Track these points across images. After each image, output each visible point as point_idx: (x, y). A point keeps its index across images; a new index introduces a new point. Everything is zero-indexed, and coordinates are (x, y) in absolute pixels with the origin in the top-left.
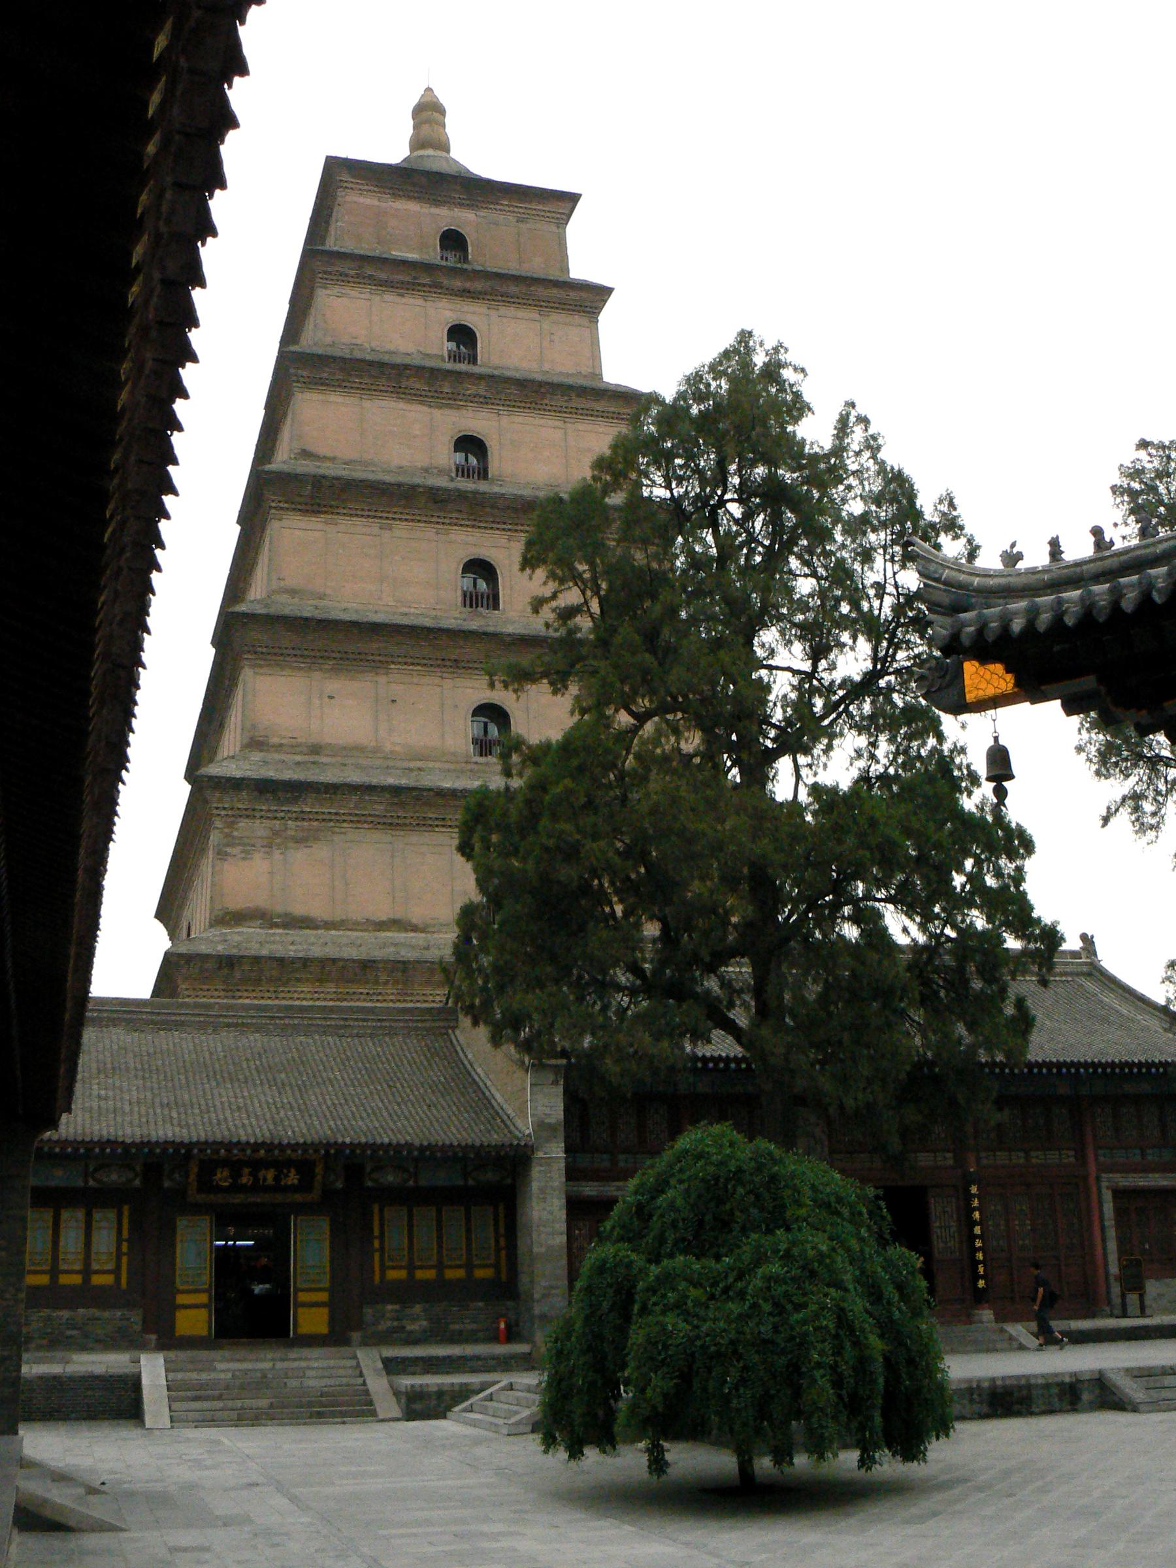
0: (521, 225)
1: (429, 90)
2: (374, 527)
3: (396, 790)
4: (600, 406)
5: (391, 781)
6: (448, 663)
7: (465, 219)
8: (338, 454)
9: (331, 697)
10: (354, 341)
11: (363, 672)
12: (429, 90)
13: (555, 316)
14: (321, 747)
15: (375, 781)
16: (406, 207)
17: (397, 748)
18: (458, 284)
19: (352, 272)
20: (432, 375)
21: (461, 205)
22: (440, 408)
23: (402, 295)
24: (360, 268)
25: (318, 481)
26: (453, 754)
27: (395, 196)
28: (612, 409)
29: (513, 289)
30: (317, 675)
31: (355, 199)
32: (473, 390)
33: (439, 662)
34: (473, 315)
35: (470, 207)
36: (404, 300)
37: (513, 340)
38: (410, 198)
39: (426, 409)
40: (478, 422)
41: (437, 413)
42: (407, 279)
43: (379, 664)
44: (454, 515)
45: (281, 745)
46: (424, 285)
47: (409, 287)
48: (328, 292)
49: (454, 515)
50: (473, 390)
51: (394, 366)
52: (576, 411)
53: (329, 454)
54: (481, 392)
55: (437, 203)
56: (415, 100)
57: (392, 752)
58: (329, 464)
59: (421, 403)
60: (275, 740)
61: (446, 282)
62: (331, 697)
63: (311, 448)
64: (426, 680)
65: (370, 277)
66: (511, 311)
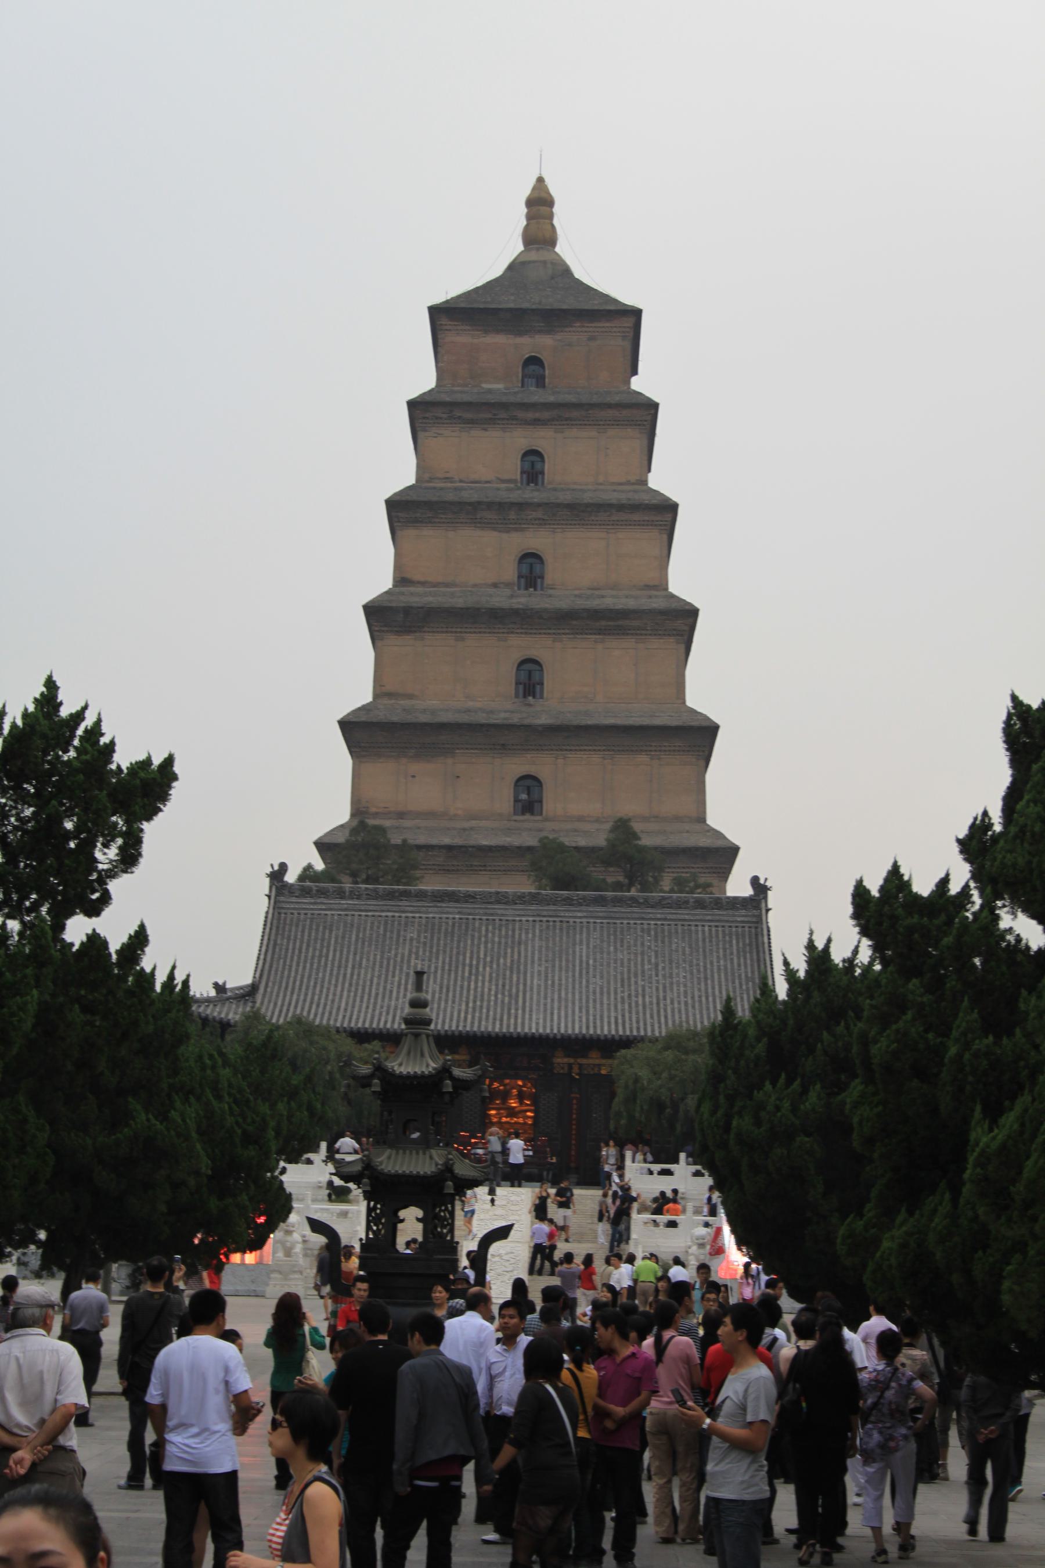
1: (540, 180)
3: (450, 848)
4: (636, 517)
5: (447, 841)
7: (542, 344)
9: (413, 776)
10: (448, 475)
12: (540, 180)
15: (434, 841)
17: (460, 812)
18: (530, 415)
20: (501, 507)
21: (540, 332)
22: (508, 532)
23: (485, 430)
25: (407, 611)
27: (486, 332)
28: (646, 518)
29: (575, 414)
34: (543, 439)
35: (549, 332)
37: (577, 461)
38: (498, 332)
39: (496, 534)
40: (537, 540)
41: (505, 536)
42: (490, 416)
45: (377, 813)
46: (503, 419)
47: (492, 422)
48: (427, 434)
51: (470, 504)
53: (422, 579)
55: (520, 333)
56: (526, 190)
58: (420, 589)
59: (494, 529)
60: (373, 810)
61: (521, 414)
62: (413, 776)
63: (408, 576)
65: (460, 417)
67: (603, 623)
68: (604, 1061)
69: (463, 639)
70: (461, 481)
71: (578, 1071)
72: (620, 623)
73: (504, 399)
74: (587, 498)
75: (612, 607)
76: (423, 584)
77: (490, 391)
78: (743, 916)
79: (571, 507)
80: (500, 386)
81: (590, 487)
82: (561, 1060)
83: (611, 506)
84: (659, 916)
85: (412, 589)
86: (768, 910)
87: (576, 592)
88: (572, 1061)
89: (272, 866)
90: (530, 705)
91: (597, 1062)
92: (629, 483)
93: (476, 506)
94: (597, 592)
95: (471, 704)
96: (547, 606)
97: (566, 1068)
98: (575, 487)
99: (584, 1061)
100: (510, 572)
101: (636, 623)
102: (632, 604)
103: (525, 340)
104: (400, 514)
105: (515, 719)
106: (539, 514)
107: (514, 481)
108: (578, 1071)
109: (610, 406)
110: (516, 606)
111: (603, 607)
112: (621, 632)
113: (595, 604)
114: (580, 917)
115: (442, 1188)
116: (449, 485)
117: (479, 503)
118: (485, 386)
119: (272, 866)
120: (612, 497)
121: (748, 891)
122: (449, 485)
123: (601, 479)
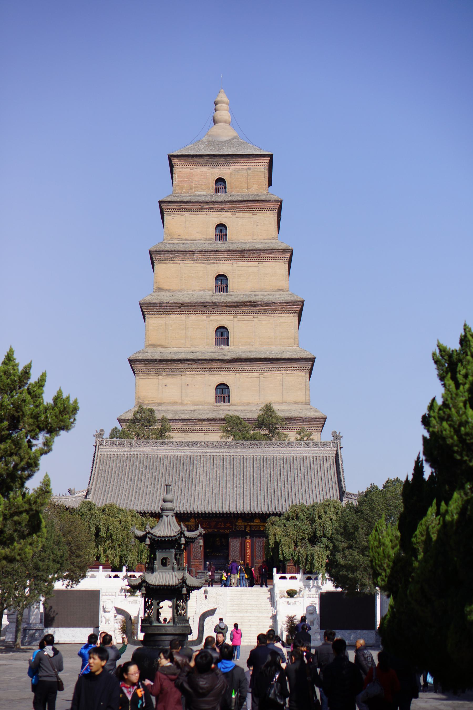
0: (248, 171)
2: (182, 317)
3: (184, 420)
4: (272, 255)
5: (183, 417)
6: (207, 370)
8: (171, 288)
11: (177, 375)
13: (259, 214)
14: (162, 403)
16: (201, 170)
17: (189, 402)
19: (178, 208)
22: (209, 264)
23: (198, 214)
24: (181, 205)
26: (208, 403)
28: (277, 256)
29: (241, 205)
30: (161, 377)
31: (180, 170)
32: (222, 256)
33: (204, 370)
36: (198, 216)
40: (223, 267)
41: (208, 266)
42: (200, 207)
43: (183, 372)
44: (212, 310)
45: (148, 404)
47: (201, 210)
48: (169, 217)
49: (212, 310)
50: (222, 256)
51: (191, 251)
52: (264, 259)
53: (168, 288)
54: (226, 256)
55: (214, 166)
57: (187, 404)
58: (168, 293)
59: (203, 263)
60: (146, 402)
64: (199, 376)
65: (185, 209)
66: (241, 214)
67: (257, 308)
68: (262, 524)
69: (189, 317)
70: (186, 240)
71: (249, 529)
72: (266, 308)
73: (207, 199)
74: (248, 247)
75: (261, 300)
76: (169, 291)
77: (199, 196)
78: (329, 451)
79: (241, 251)
80: (204, 193)
81: (249, 241)
82: (240, 523)
83: (260, 250)
84: (288, 452)
85: (163, 293)
86: (341, 448)
87: (244, 293)
88: (246, 524)
89: (97, 431)
90: (222, 349)
91: (258, 524)
92: (268, 239)
93: (192, 252)
94: (253, 293)
95: (193, 349)
96: (230, 300)
97: (243, 528)
98: (242, 241)
99: (252, 524)
100: (211, 283)
101: (273, 308)
102: (271, 299)
103: (216, 170)
104: (157, 257)
105: (214, 356)
106: (225, 255)
107: (213, 239)
108: (249, 529)
109: (258, 201)
110: (214, 300)
111: (257, 300)
112: (266, 312)
113: (253, 299)
114: (249, 453)
115: (181, 591)
116: (180, 242)
117: (195, 250)
118: (198, 193)
119: (97, 431)
120: (261, 247)
121: (331, 439)
122: (180, 242)
123: (255, 237)
